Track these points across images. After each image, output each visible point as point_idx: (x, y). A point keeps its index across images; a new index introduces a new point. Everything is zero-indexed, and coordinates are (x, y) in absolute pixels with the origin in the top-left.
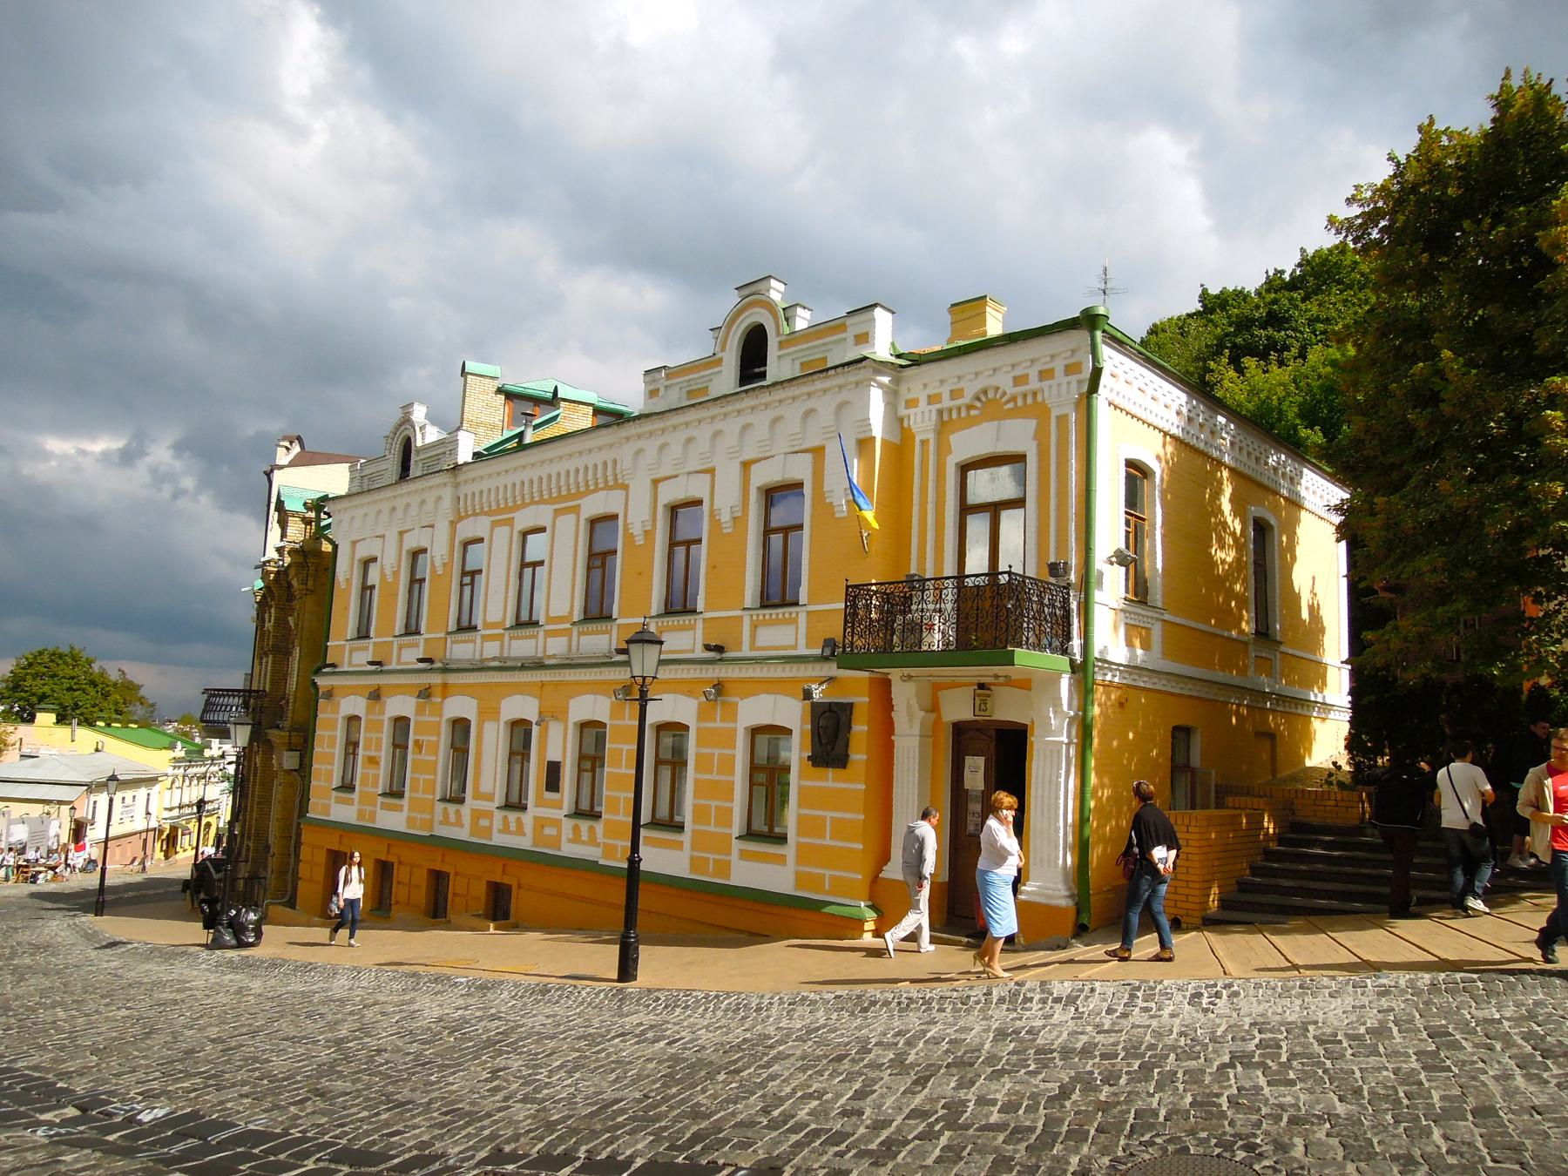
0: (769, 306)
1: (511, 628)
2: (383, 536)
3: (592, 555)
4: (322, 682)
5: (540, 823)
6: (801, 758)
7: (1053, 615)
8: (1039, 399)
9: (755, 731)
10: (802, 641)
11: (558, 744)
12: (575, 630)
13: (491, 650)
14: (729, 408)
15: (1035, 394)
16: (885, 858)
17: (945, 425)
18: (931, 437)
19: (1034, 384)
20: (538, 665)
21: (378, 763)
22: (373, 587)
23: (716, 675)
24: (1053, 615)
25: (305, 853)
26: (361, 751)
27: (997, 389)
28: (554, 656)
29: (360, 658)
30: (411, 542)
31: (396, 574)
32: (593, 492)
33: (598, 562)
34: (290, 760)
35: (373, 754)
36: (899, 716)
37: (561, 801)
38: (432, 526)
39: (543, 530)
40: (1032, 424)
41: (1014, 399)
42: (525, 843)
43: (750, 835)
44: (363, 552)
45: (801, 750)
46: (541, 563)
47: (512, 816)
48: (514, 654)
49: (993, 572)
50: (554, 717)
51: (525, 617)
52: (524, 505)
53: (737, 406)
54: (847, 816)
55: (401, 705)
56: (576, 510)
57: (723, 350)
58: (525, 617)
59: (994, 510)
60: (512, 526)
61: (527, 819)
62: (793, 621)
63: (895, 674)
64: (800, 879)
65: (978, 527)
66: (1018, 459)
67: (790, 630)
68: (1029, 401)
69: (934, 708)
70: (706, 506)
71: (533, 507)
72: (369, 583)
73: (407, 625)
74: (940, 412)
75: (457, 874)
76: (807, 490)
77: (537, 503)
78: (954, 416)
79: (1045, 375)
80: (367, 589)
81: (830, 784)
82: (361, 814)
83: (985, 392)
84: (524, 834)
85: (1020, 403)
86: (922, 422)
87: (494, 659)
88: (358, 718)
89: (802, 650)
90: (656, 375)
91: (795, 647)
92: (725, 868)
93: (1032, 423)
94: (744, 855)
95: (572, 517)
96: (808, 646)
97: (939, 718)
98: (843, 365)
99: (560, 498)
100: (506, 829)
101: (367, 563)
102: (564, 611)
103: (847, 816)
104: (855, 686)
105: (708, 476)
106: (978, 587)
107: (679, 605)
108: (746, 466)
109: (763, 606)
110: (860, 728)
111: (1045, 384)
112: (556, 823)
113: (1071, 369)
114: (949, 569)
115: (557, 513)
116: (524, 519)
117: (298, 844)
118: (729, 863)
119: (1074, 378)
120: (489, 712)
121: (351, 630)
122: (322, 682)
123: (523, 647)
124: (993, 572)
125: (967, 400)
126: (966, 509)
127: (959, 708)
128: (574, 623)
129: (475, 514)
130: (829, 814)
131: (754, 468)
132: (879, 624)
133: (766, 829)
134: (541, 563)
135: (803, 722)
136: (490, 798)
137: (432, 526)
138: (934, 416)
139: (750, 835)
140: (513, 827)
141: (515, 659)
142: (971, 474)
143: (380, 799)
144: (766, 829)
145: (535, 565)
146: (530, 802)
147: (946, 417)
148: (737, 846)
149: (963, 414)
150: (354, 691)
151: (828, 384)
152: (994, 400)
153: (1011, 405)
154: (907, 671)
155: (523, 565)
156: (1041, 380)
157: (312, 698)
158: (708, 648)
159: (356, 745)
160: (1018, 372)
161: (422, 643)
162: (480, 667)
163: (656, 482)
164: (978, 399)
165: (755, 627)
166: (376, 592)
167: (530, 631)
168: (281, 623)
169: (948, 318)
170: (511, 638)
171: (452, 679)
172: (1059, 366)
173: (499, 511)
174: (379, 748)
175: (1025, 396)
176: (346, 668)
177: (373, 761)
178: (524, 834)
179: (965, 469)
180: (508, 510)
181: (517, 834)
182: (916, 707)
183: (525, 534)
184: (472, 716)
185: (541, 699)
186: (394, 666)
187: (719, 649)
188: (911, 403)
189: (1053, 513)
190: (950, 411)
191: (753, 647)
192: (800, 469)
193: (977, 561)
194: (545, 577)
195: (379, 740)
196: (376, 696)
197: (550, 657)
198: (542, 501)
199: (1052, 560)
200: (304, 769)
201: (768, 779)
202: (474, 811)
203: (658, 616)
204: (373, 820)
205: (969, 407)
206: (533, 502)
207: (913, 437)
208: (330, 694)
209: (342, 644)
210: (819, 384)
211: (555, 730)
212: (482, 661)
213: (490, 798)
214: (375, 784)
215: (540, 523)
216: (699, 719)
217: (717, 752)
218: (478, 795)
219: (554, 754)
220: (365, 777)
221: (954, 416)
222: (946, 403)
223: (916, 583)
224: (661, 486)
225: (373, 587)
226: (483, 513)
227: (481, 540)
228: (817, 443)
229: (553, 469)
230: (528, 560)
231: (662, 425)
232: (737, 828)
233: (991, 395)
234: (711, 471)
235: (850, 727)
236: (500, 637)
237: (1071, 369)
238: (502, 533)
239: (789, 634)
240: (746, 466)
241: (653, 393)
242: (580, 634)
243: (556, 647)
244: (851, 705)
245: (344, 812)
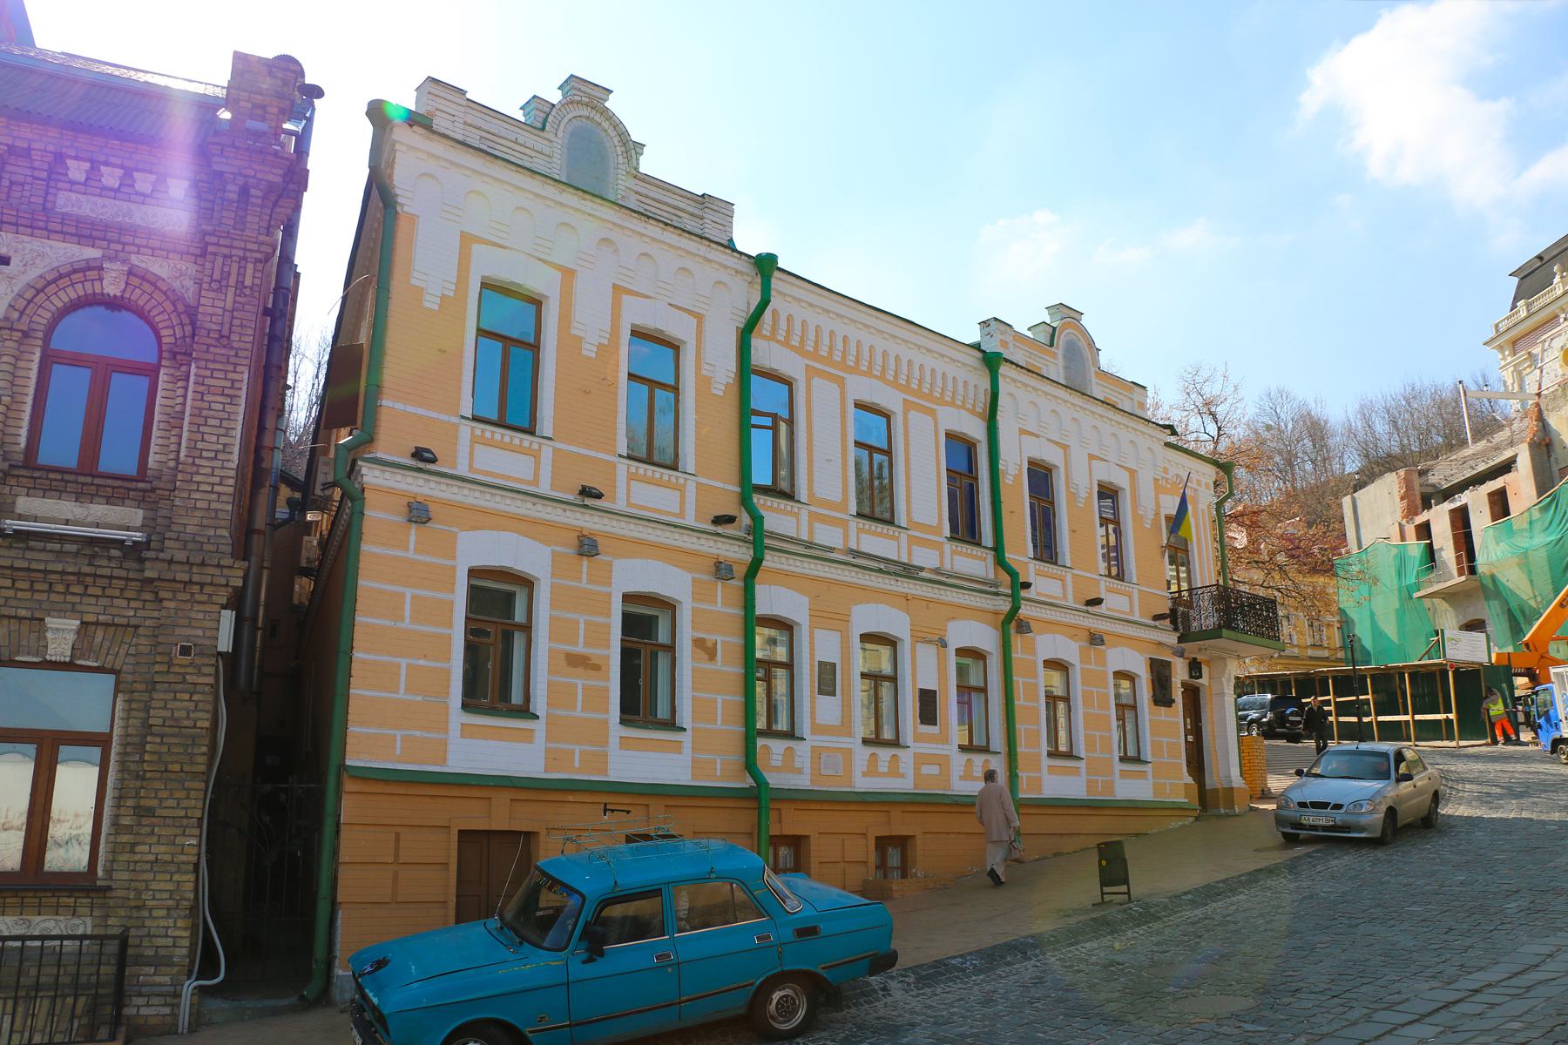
20: (908, 571)
42: (904, 784)
47: (884, 754)
53: (1093, 408)
82: (552, 758)
92: (1110, 785)
100: (872, 771)
112: (943, 762)
118: (1112, 782)
120: (831, 617)
146: (908, 734)
178: (903, 776)
181: (897, 774)
204: (605, 771)
218: (817, 729)
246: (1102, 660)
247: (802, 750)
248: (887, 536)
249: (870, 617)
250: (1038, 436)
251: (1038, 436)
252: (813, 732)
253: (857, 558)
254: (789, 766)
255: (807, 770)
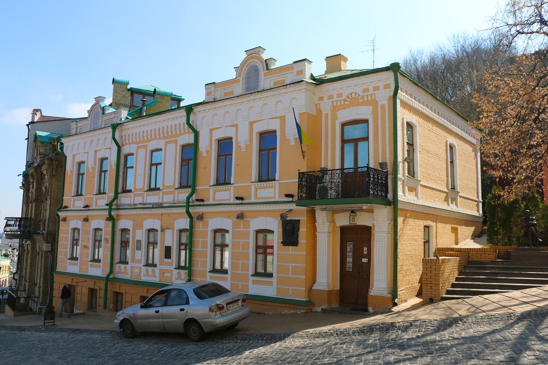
0: (260, 59)
1: (147, 191)
2: (88, 153)
3: (182, 160)
4: (62, 214)
5: (162, 272)
6: (278, 243)
7: (382, 183)
8: (373, 98)
9: (258, 232)
10: (277, 196)
11: (170, 239)
12: (176, 191)
13: (138, 200)
14: (244, 100)
15: (371, 95)
16: (314, 281)
17: (335, 109)
18: (329, 112)
19: (371, 92)
20: (160, 206)
21: (88, 248)
22: (83, 174)
23: (240, 209)
24: (382, 183)
25: (56, 286)
26: (80, 243)
27: (356, 93)
28: (167, 203)
29: (79, 203)
30: (100, 155)
31: (93, 169)
32: (183, 134)
33: (186, 163)
34: (46, 247)
35: (86, 244)
36: (319, 224)
37: (172, 262)
38: (110, 148)
39: (161, 150)
40: (370, 108)
41: (363, 97)
42: (156, 280)
43: (256, 274)
44: (78, 159)
45: (278, 239)
46: (160, 164)
47: (150, 269)
48: (149, 201)
49: (356, 167)
50: (168, 228)
51: (153, 186)
52: (152, 140)
53: (247, 99)
54: (298, 265)
55: (95, 224)
56: (176, 142)
57: (240, 76)
58: (153, 186)
59: (356, 141)
60: (146, 149)
61: (157, 270)
62: (274, 187)
63: (318, 208)
64: (278, 290)
65: (349, 148)
66: (366, 121)
67: (272, 190)
68: (369, 98)
69: (333, 221)
70: (234, 141)
71: (156, 141)
72: (81, 172)
73: (99, 190)
74: (333, 102)
75: (126, 293)
76: (278, 134)
77: (158, 139)
78: (339, 104)
79: (376, 88)
80: (80, 175)
81: (291, 252)
82: (81, 269)
83: (351, 94)
84: (156, 277)
85: (365, 99)
86: (326, 107)
87: (140, 204)
88: (78, 229)
89: (277, 199)
90: (210, 86)
91: (274, 197)
93: (370, 108)
94: (254, 282)
95: (174, 145)
96: (279, 197)
97: (335, 225)
98: (293, 83)
99: (168, 137)
100: (147, 275)
101: (80, 164)
102: (172, 184)
103: (298, 265)
104: (299, 213)
105: (234, 128)
106: (363, 172)
107: (223, 180)
108: (251, 124)
109: (260, 181)
110: (303, 230)
111: (376, 92)
112: (171, 272)
113: (387, 86)
114: (338, 166)
115: (167, 143)
116: (152, 145)
117: (52, 282)
118: (248, 285)
119: (387, 90)
120: (138, 226)
121: (73, 192)
122: (62, 214)
123: (153, 198)
124: (356, 167)
125: (344, 97)
126: (344, 142)
127: (343, 220)
128: (176, 189)
129: (130, 144)
130: (291, 265)
131: (254, 125)
132: (311, 188)
133: (263, 271)
134: (160, 164)
135: (278, 228)
136: (140, 261)
137: (110, 148)
138: (330, 104)
139: (256, 274)
140: (151, 274)
141: (150, 204)
142: (346, 127)
143: (90, 263)
144: (263, 271)
145: (157, 164)
147: (335, 104)
148: (251, 279)
149: (342, 103)
150: (77, 218)
151: (286, 90)
152: (355, 98)
153: (362, 100)
154: (324, 206)
155: (152, 165)
156: (374, 91)
157: (56, 221)
158: (237, 198)
159: (77, 240)
160: (365, 87)
161: (107, 198)
162: (134, 207)
163: (211, 130)
164: (348, 97)
165: (256, 189)
166: (85, 176)
167: (156, 192)
168: (39, 189)
169: (325, 63)
170: (147, 195)
171: (121, 212)
172: (381, 85)
173: (140, 142)
174: (88, 242)
175: (367, 96)
176: (72, 208)
177: (86, 247)
178: (156, 277)
179: (344, 125)
180: (144, 141)
182: (326, 221)
183: (152, 152)
184: (130, 227)
185: (161, 221)
186: (94, 208)
187: (242, 199)
188: (321, 99)
189: (380, 143)
190: (337, 101)
191: (256, 198)
192: (274, 125)
193: (349, 164)
194: (162, 169)
195: (88, 238)
196: (86, 220)
197: (165, 203)
198: (160, 138)
199: (380, 162)
200: (53, 252)
201: (263, 250)
202: (132, 268)
203: (214, 185)
204: (87, 273)
205: (345, 100)
206: (156, 138)
207: (322, 112)
208: (65, 220)
209: (69, 199)
210: (283, 90)
211: (168, 233)
212: (135, 205)
213: (140, 261)
214: (87, 257)
215: (159, 147)
216: (233, 228)
217: (241, 241)
219: (168, 244)
220: (81, 253)
221: (339, 104)
222: (335, 98)
223: (324, 171)
224: (214, 132)
225: (83, 174)
226: (133, 143)
227: (132, 154)
228: (283, 115)
229: (165, 124)
230: (153, 163)
231: (214, 107)
232: (251, 271)
233: (353, 95)
234: (236, 126)
235: (299, 229)
236: (142, 195)
237: (387, 86)
238: (142, 152)
239: (270, 191)
240: (251, 124)
241: (208, 94)
242: (178, 193)
243: (168, 199)
244: (299, 220)
245: (73, 268)
246: (248, 225)
247: (128, 267)
248: (154, 195)
249: (149, 224)
250: (220, 128)
251: (220, 128)
252: (132, 262)
253: (144, 206)
254: (124, 272)
255: (129, 274)
